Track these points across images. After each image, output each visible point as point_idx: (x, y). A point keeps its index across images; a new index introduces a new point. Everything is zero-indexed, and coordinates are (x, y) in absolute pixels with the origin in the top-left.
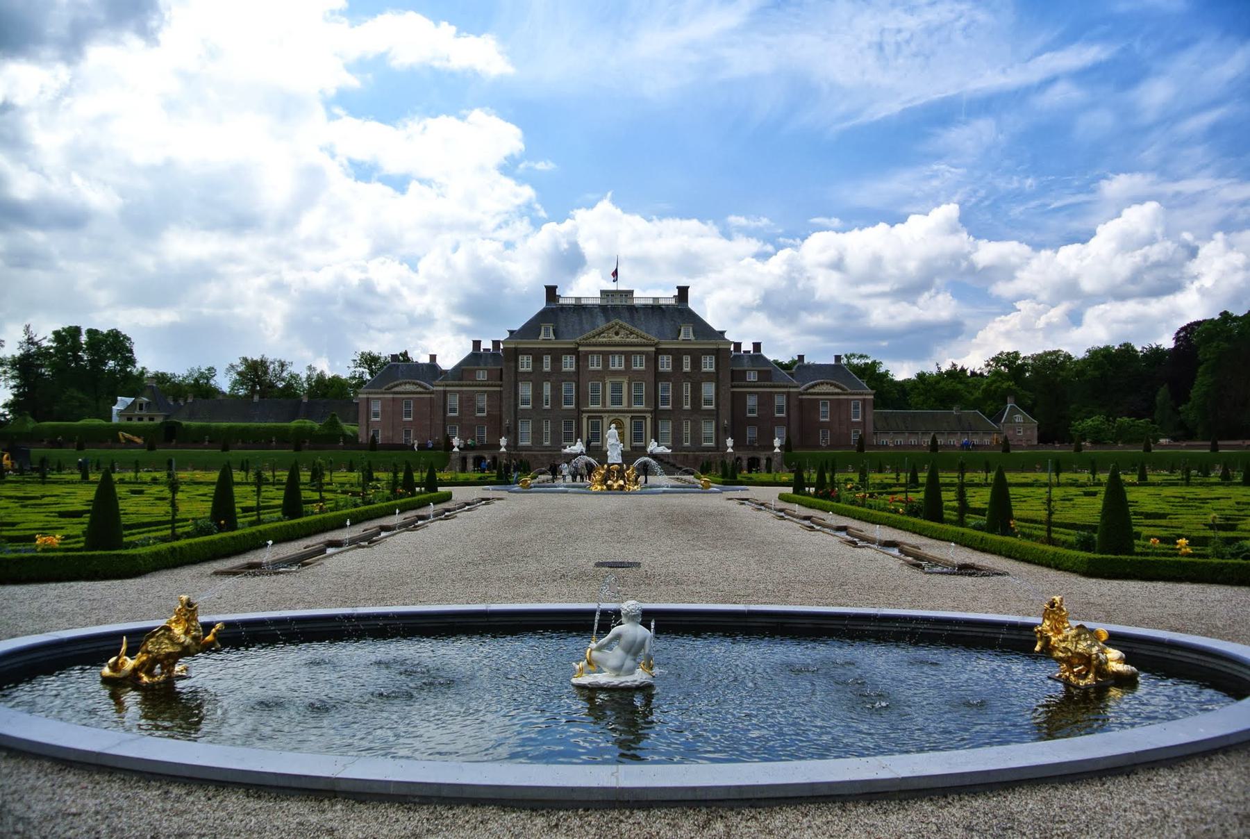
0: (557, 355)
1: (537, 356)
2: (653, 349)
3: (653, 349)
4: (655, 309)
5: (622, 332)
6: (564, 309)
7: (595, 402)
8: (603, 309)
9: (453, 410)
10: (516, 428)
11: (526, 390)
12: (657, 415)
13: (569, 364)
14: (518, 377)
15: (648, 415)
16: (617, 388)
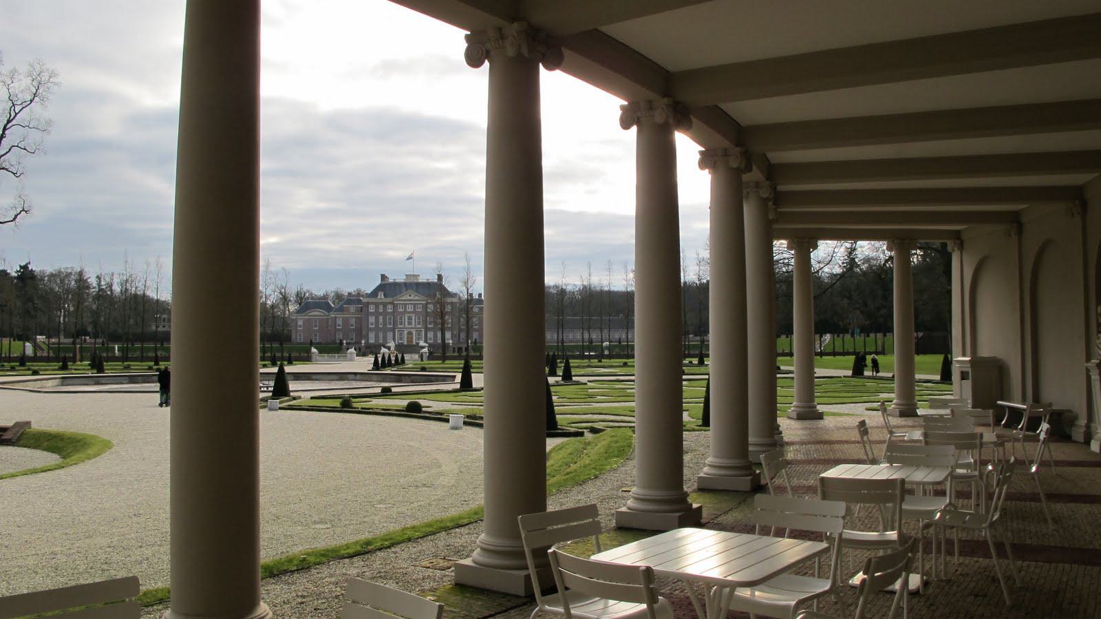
0: (385, 305)
1: (377, 305)
2: (425, 302)
3: (425, 302)
4: (428, 285)
5: (412, 296)
6: (391, 284)
7: (401, 324)
8: (405, 284)
9: (339, 326)
10: (368, 335)
11: (372, 319)
12: (427, 329)
13: (390, 309)
14: (369, 314)
15: (423, 330)
16: (410, 318)
